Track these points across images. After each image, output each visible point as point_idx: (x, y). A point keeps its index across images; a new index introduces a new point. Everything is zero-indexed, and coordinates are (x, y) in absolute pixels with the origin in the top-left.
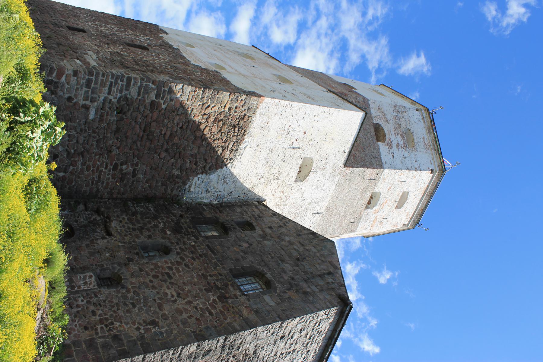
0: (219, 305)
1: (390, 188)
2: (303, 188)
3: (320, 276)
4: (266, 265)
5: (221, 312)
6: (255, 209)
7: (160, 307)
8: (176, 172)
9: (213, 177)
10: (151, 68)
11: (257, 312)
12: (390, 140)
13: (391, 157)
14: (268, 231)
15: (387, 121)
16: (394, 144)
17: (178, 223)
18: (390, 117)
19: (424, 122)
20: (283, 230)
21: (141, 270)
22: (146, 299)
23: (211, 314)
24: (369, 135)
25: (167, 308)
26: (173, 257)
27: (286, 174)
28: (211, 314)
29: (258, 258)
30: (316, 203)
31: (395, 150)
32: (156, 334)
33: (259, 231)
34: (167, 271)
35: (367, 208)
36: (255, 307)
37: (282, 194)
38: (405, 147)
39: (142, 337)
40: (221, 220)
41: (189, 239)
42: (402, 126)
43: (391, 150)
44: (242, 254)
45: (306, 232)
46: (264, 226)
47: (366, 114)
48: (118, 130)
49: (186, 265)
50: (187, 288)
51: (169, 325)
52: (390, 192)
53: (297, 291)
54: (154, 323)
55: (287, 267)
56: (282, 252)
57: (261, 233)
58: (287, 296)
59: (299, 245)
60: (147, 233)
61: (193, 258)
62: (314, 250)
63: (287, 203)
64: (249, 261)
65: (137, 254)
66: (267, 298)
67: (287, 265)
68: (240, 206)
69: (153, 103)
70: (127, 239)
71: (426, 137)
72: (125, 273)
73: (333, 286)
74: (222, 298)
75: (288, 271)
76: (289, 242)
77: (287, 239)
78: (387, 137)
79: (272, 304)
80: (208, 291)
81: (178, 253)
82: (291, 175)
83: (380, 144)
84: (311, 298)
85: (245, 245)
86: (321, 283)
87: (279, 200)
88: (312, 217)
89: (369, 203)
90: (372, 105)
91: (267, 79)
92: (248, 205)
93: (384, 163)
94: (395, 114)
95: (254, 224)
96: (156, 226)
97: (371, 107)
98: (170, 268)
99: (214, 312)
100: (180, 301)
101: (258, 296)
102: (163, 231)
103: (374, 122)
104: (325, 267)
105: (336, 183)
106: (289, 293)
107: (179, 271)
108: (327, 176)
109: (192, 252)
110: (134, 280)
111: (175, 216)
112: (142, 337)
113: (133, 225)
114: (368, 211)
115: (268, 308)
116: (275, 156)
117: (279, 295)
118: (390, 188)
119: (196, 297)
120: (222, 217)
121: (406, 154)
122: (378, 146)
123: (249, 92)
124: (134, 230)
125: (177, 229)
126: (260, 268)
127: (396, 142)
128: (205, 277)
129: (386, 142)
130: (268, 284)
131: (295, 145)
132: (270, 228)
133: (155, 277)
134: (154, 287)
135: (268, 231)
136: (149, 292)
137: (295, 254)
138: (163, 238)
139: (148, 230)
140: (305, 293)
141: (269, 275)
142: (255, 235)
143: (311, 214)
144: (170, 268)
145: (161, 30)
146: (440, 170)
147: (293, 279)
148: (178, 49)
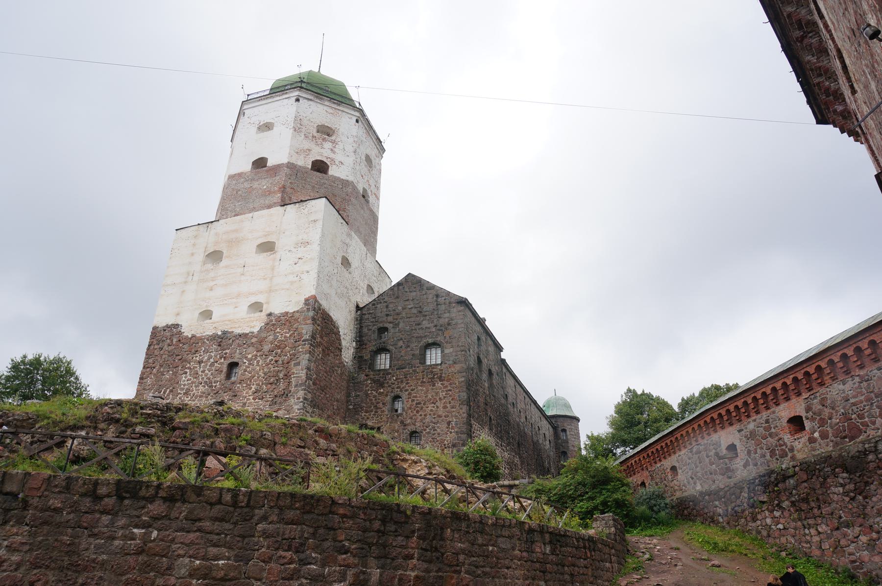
0: (445, 382)
3: (437, 305)
4: (421, 337)
5: (451, 384)
6: (366, 317)
7: (440, 416)
8: (339, 372)
9: (344, 343)
10: (281, 375)
11: (455, 363)
14: (390, 319)
15: (309, 150)
16: (332, 155)
17: (374, 381)
18: (307, 144)
20: (391, 306)
21: (411, 418)
22: (432, 422)
23: (450, 390)
25: (441, 412)
26: (404, 395)
28: (450, 390)
29: (414, 339)
31: (339, 157)
32: (456, 424)
33: (390, 326)
34: (414, 403)
35: (368, 202)
36: (451, 362)
39: (457, 432)
40: (374, 349)
41: (390, 379)
43: (337, 163)
44: (409, 349)
45: (396, 289)
46: (384, 319)
48: (322, 409)
49: (412, 390)
50: (430, 396)
51: (452, 416)
53: (446, 329)
54: (449, 423)
55: (425, 324)
56: (412, 319)
57: (391, 325)
58: (448, 338)
59: (407, 303)
60: (381, 404)
61: (407, 383)
62: (414, 294)
64: (416, 346)
65: (398, 416)
66: (447, 351)
67: (424, 322)
68: (361, 327)
69: (314, 384)
70: (384, 418)
71: (326, 108)
72: (411, 428)
73: (447, 301)
74: (441, 379)
75: (428, 326)
76: (403, 309)
77: (400, 308)
78: (325, 160)
79: (451, 350)
80: (434, 385)
81: (401, 391)
84: (454, 322)
85: (401, 343)
86: (443, 307)
89: (364, 196)
90: (293, 161)
91: (273, 269)
92: (361, 320)
93: (347, 178)
95: (381, 325)
96: (375, 396)
98: (413, 401)
99: (449, 388)
100: (438, 404)
101: (443, 356)
102: (380, 394)
103: (310, 167)
104: (430, 296)
106: (446, 334)
107: (416, 397)
109: (402, 382)
110: (418, 424)
111: (366, 380)
112: (457, 432)
113: (372, 411)
115: (454, 354)
116: (339, 291)
117: (447, 342)
119: (437, 393)
120: (371, 347)
123: (305, 304)
124: (376, 412)
125: (382, 385)
126: (422, 343)
128: (423, 382)
130: (435, 344)
132: (387, 315)
133: (418, 412)
134: (425, 415)
135: (390, 319)
136: (428, 419)
137: (415, 311)
138: (387, 395)
139: (378, 403)
140: (449, 324)
141: (430, 341)
142: (392, 331)
144: (413, 401)
145: (167, 326)
147: (436, 326)
148: (225, 333)
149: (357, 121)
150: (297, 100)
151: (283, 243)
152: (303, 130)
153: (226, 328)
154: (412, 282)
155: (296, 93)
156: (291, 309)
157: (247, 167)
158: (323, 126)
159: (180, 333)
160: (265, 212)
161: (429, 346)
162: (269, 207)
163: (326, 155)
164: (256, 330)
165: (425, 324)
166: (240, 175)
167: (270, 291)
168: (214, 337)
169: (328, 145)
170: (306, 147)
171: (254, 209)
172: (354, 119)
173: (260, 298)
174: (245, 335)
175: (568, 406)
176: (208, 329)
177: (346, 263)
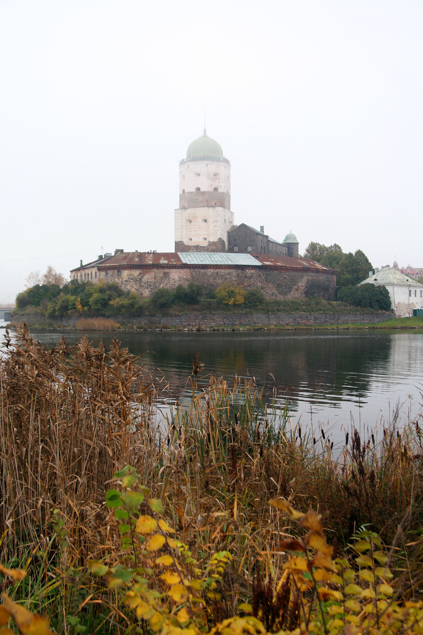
55: (247, 239)
150: (207, 165)
151: (210, 220)
153: (198, 244)
154: (243, 226)
155: (206, 162)
156: (215, 241)
157: (194, 190)
159: (184, 244)
160: (203, 208)
161: (248, 246)
162: (204, 207)
164: (206, 245)
165: (247, 239)
166: (192, 193)
167: (208, 235)
168: (194, 246)
169: (217, 180)
171: (199, 207)
173: (206, 237)
174: (203, 247)
175: (295, 238)
176: (192, 244)
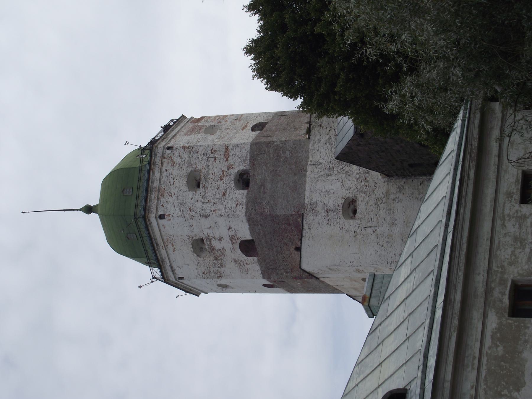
1: (224, 194)
2: (344, 191)
12: (233, 244)
13: (233, 227)
16: (227, 239)
19: (172, 267)
24: (266, 245)
27: (370, 204)
30: (322, 175)
37: (367, 184)
38: (210, 239)
42: (212, 258)
47: (300, 267)
52: (221, 189)
63: (358, 176)
78: (237, 246)
82: (364, 203)
83: (249, 238)
87: (368, 179)
88: (321, 161)
94: (222, 270)
97: (260, 272)
105: (306, 198)
108: (320, 205)
114: (242, 168)
118: (224, 194)
121: (209, 231)
122: (251, 235)
127: (223, 242)
129: (239, 241)
131: (370, 230)
143: (323, 165)
146: (149, 220)
149: (162, 217)
152: (216, 270)
158: (195, 251)
163: (230, 245)
170: (233, 264)
172: (161, 222)
177: (350, 208)
